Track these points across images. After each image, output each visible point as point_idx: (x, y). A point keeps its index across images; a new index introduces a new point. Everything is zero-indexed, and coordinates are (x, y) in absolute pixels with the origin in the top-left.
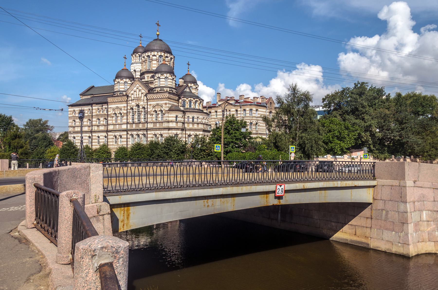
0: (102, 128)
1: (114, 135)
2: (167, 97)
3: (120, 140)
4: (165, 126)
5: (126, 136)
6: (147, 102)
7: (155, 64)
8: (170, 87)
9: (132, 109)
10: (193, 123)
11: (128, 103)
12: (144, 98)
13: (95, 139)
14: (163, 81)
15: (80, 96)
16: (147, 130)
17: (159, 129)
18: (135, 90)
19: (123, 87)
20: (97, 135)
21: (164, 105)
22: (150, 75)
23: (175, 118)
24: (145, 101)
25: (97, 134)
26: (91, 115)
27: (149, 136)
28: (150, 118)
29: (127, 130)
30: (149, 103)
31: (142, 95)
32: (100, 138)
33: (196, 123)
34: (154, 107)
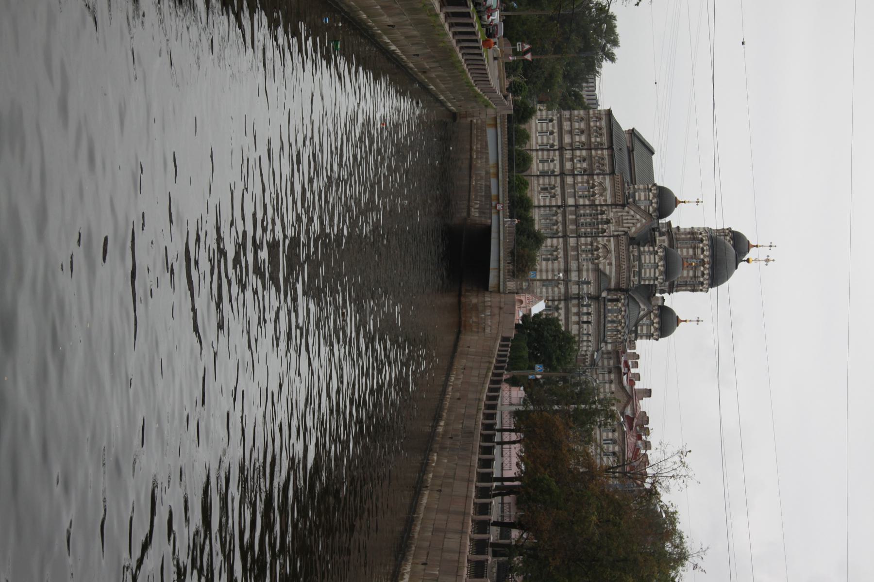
0: (568, 165)
1: (556, 185)
2: (621, 265)
3: (548, 196)
4: (572, 264)
5: (554, 203)
6: (613, 236)
7: (688, 252)
8: (640, 272)
9: (602, 213)
10: (579, 314)
12: (621, 231)
13: (549, 155)
14: (650, 261)
16: (565, 236)
19: (642, 198)
20: (555, 158)
21: (608, 261)
22: (666, 244)
24: (616, 233)
25: (557, 158)
27: (555, 240)
30: (612, 239)
31: (625, 227)
33: (579, 319)
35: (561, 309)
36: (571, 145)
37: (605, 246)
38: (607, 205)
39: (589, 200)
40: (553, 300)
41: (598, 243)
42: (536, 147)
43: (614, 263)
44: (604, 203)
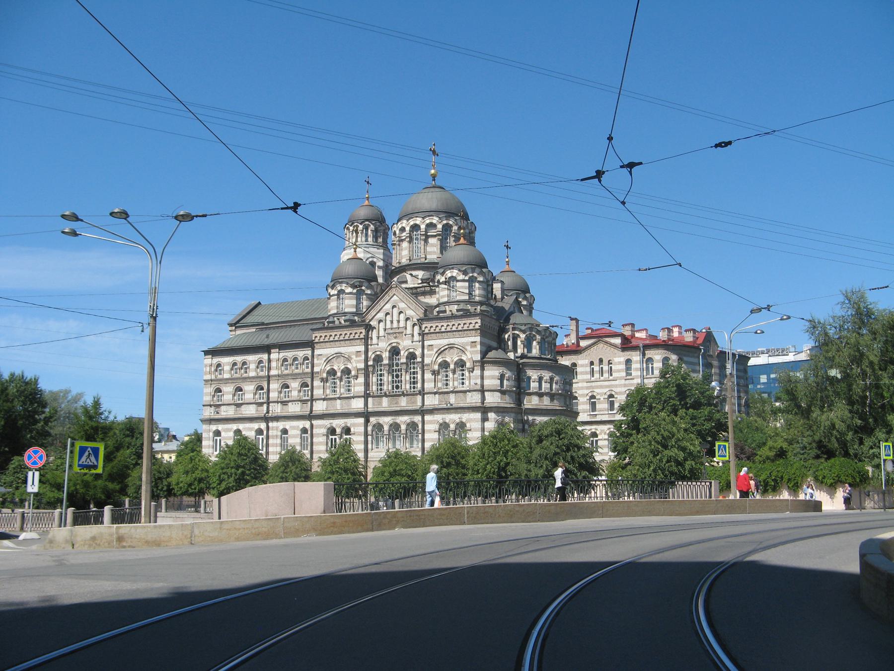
0: (294, 408)
6: (423, 341)
9: (378, 359)
11: (369, 343)
15: (230, 328)
16: (422, 412)
18: (387, 309)
21: (468, 348)
23: (499, 381)
24: (417, 337)
25: (281, 425)
29: (366, 415)
30: (426, 343)
32: (289, 433)
44: (363, 356)
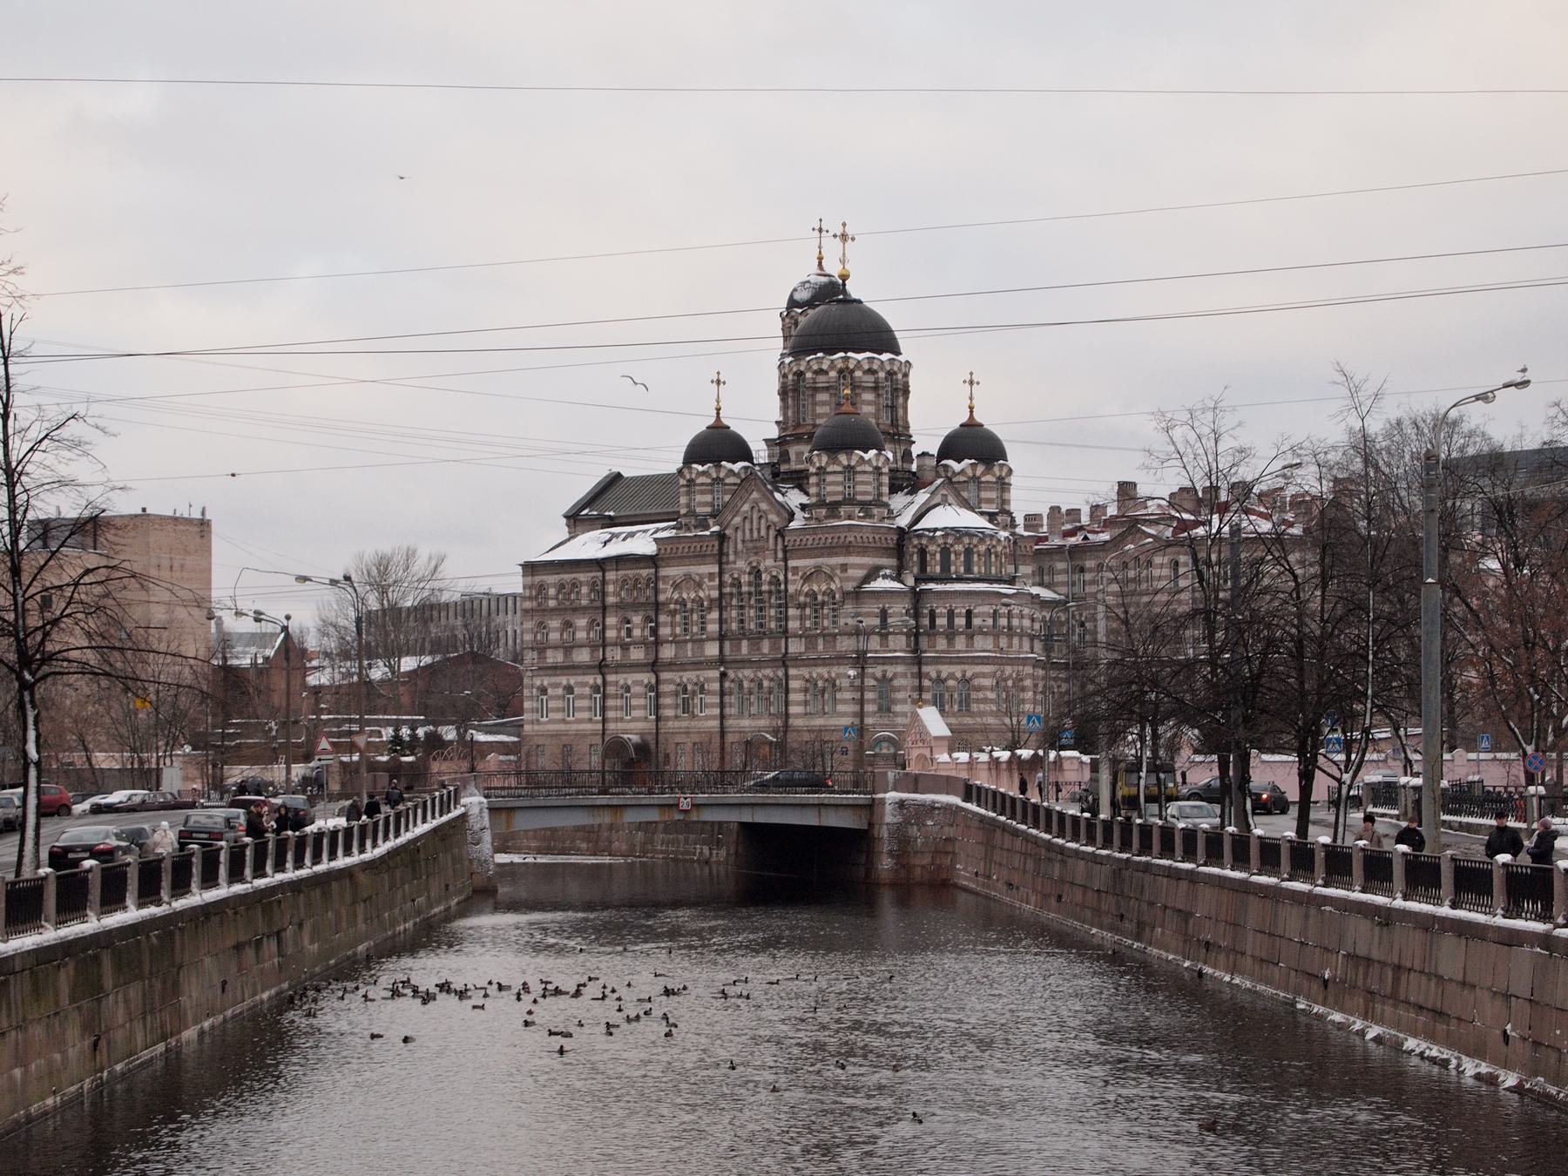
0: (637, 654)
5: (716, 686)
6: (785, 560)
7: (824, 403)
9: (737, 583)
12: (776, 544)
17: (824, 662)
19: (708, 498)
20: (622, 682)
21: (838, 572)
24: (780, 555)
25: (621, 678)
26: (599, 604)
27: (793, 684)
28: (795, 618)
30: (792, 563)
33: (962, 633)
34: (807, 578)
35: (939, 673)
36: (593, 647)
37: (807, 578)
38: (721, 573)
39: (710, 609)
40: (920, 689)
41: (799, 593)
42: (597, 722)
43: (840, 560)
